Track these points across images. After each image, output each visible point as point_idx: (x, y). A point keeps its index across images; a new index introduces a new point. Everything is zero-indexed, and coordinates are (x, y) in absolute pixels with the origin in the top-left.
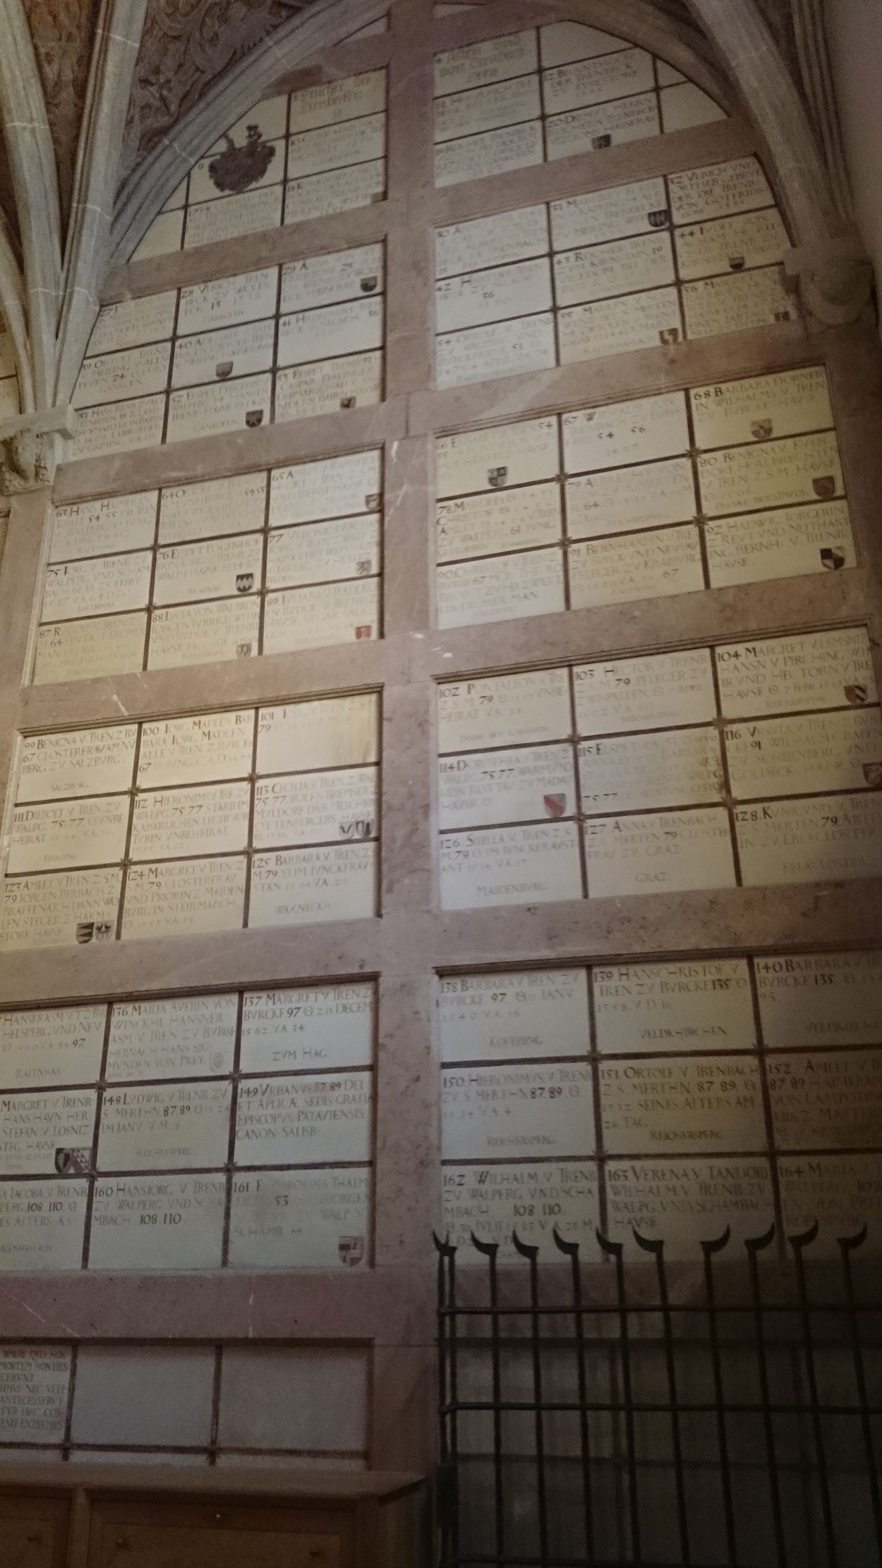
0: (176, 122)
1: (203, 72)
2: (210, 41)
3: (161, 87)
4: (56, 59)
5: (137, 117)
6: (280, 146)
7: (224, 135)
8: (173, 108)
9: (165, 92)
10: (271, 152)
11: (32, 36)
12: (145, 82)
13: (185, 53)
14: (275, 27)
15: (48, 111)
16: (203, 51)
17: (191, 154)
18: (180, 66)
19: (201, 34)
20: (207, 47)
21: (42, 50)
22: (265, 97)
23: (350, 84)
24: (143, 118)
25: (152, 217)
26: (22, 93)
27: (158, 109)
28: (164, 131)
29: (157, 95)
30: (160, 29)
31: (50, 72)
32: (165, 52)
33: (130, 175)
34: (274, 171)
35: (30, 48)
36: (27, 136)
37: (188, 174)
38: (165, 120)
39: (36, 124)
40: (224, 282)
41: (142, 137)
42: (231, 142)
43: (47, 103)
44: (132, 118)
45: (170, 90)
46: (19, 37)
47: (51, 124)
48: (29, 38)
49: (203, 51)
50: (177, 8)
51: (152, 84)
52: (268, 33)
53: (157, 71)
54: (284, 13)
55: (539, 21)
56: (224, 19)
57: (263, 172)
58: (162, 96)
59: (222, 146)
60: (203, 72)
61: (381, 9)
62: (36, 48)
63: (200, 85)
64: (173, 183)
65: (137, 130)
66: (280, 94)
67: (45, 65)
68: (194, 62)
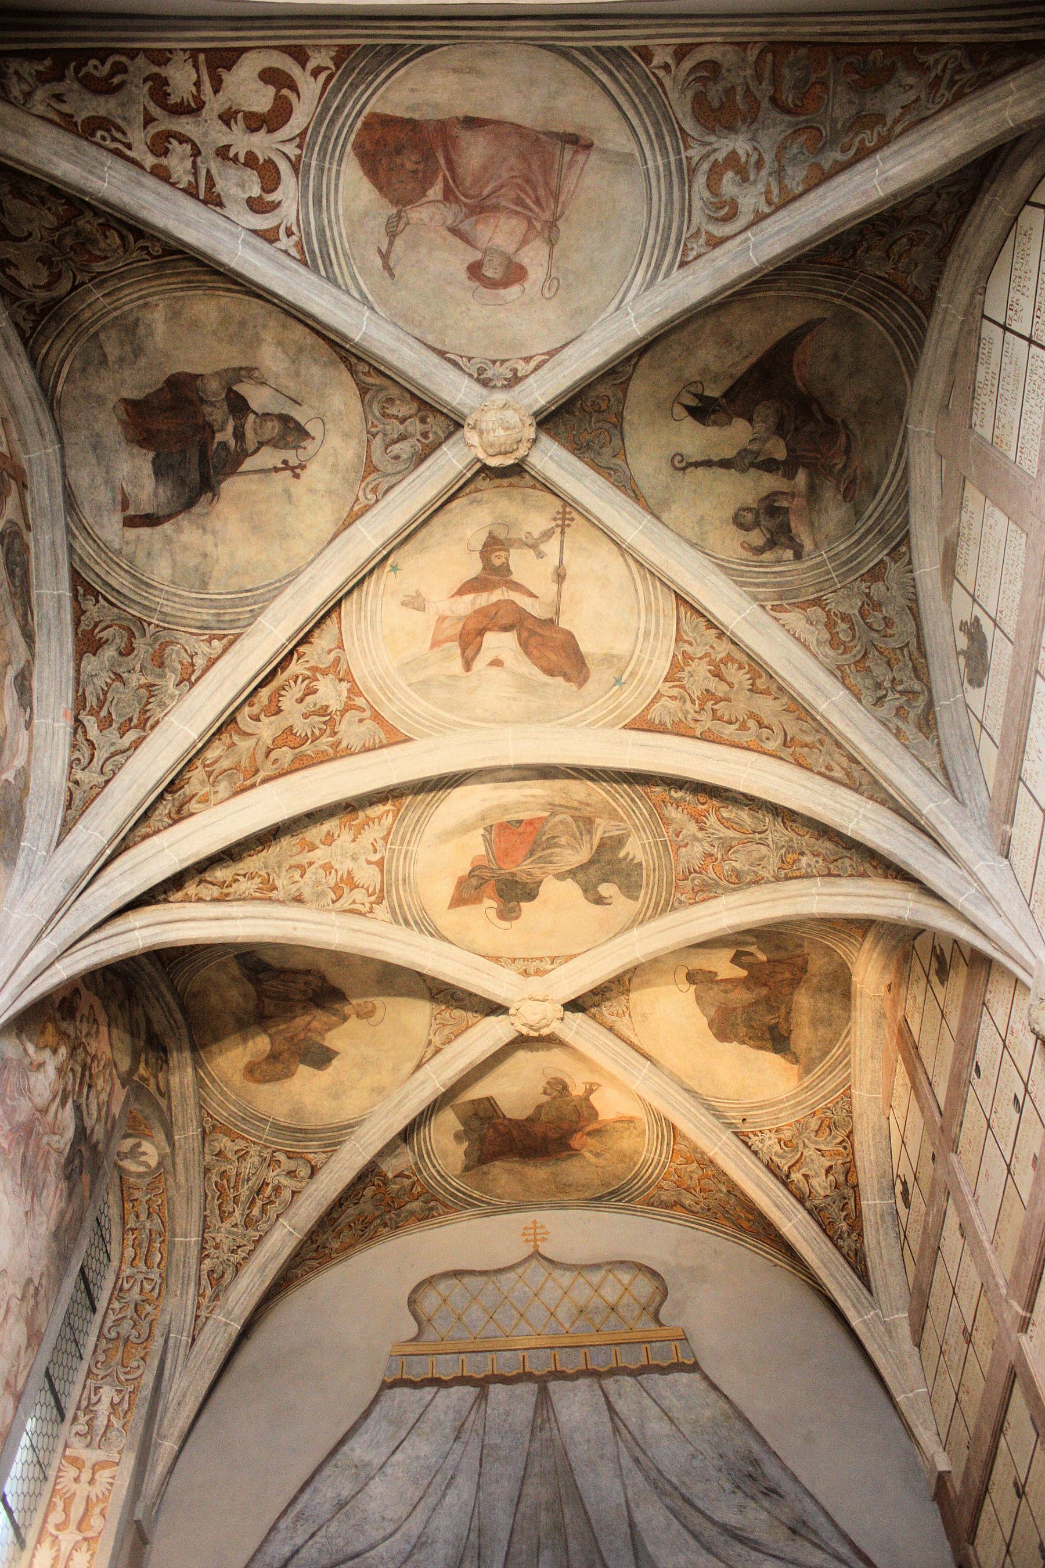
0: (930, 691)
1: (907, 644)
2: (887, 626)
3: (893, 689)
4: (832, 763)
5: (900, 724)
6: (977, 611)
7: (958, 654)
8: (917, 687)
9: (900, 688)
10: (977, 620)
11: (811, 770)
12: (879, 701)
13: (881, 653)
14: (910, 562)
15: (862, 794)
16: (891, 636)
17: (955, 693)
18: (889, 663)
19: (878, 631)
20: (889, 631)
21: (823, 770)
22: (949, 599)
23: (965, 517)
24: (905, 719)
25: (975, 760)
26: (838, 806)
27: (908, 701)
28: (930, 704)
29: (898, 695)
30: (849, 665)
31: (838, 774)
32: (869, 670)
33: (941, 757)
34: (987, 626)
35: (818, 777)
36: (863, 824)
37: (967, 706)
38: (921, 702)
39: (861, 811)
40: (1030, 734)
41: (920, 730)
42: (962, 652)
43: (856, 790)
44: (898, 729)
45: (901, 682)
46: (805, 783)
47: (871, 798)
48: (808, 774)
49: (891, 636)
50: (844, 643)
51: (885, 696)
52: (911, 571)
53: (879, 686)
54: (903, 549)
55: (977, 313)
56: (877, 606)
57: (985, 640)
58: (901, 693)
59: (962, 660)
60: (907, 644)
61: (934, 457)
62: (819, 773)
63: (916, 654)
64: (964, 724)
65: (910, 730)
66: (951, 585)
67: (832, 774)
68: (894, 649)
